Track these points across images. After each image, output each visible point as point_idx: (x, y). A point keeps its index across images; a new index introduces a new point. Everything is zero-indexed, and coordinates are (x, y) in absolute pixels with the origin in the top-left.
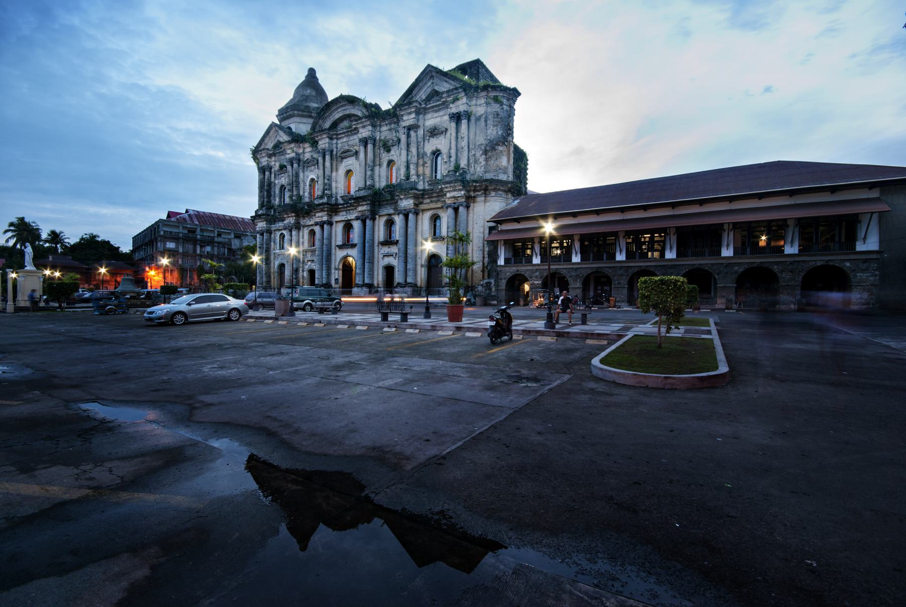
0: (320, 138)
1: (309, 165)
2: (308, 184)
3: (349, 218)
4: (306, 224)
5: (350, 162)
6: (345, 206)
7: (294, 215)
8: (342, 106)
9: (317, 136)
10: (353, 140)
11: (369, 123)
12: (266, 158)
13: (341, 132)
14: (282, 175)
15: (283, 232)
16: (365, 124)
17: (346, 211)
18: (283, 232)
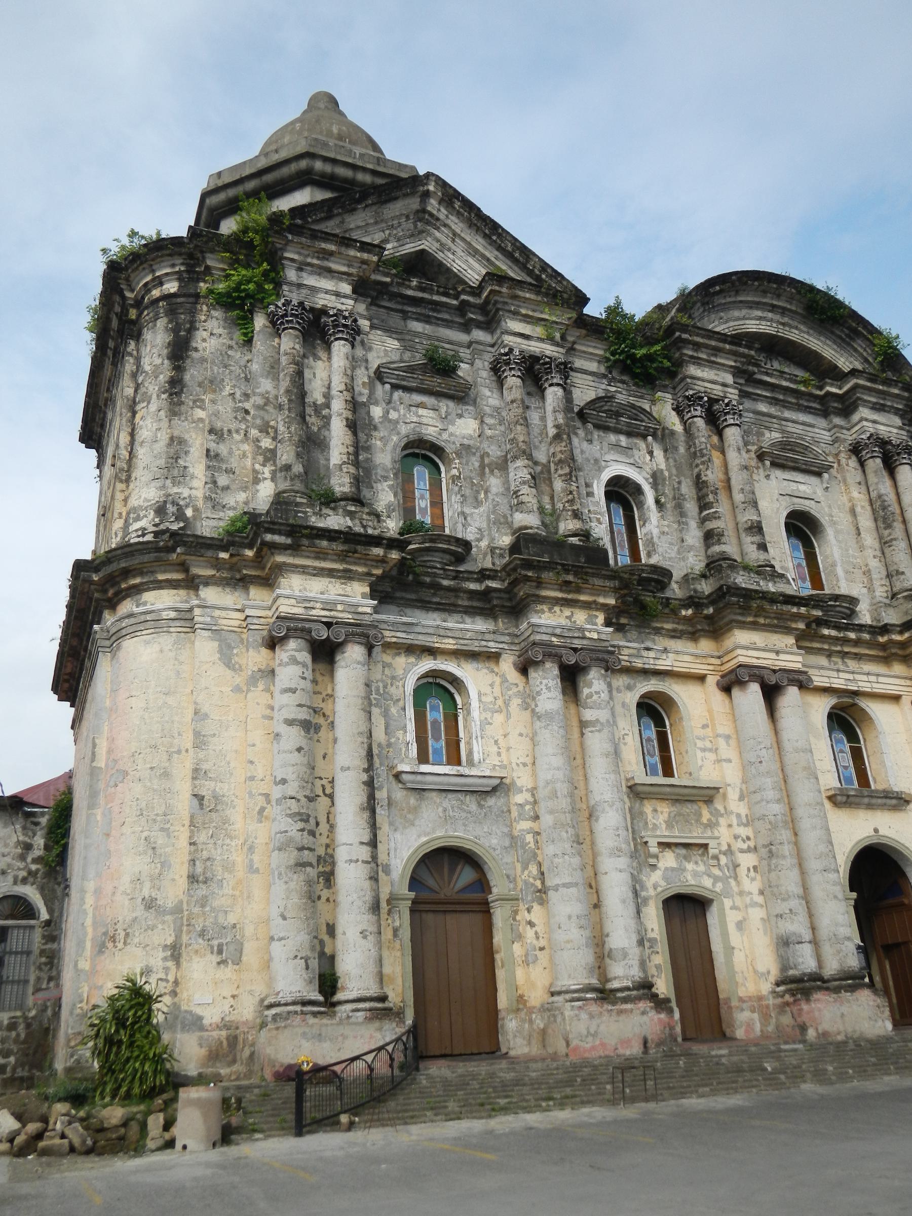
0: (704, 356)
1: (612, 423)
2: (599, 490)
3: (865, 687)
4: (638, 664)
5: (802, 488)
6: (852, 635)
7: (612, 601)
8: (774, 306)
9: (697, 346)
10: (804, 424)
11: (900, 407)
12: (346, 288)
13: (768, 379)
14: (418, 398)
15: (450, 666)
16: (889, 403)
17: (829, 656)
18: (450, 666)
